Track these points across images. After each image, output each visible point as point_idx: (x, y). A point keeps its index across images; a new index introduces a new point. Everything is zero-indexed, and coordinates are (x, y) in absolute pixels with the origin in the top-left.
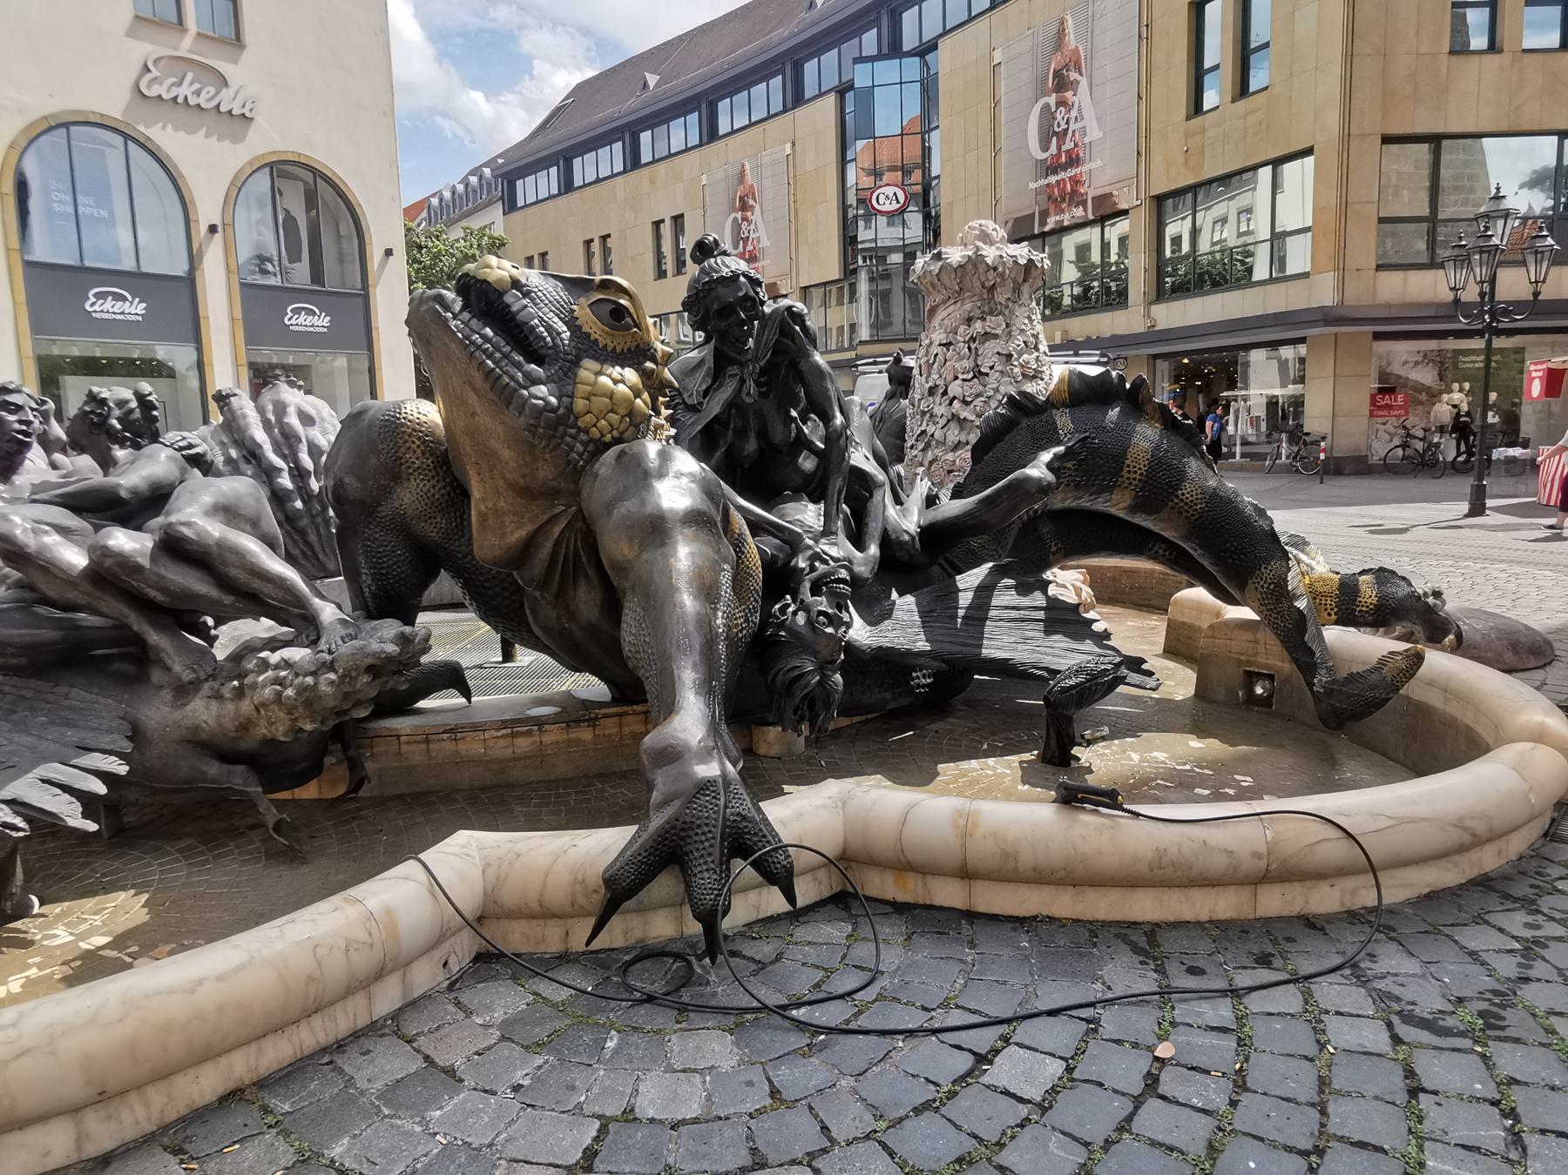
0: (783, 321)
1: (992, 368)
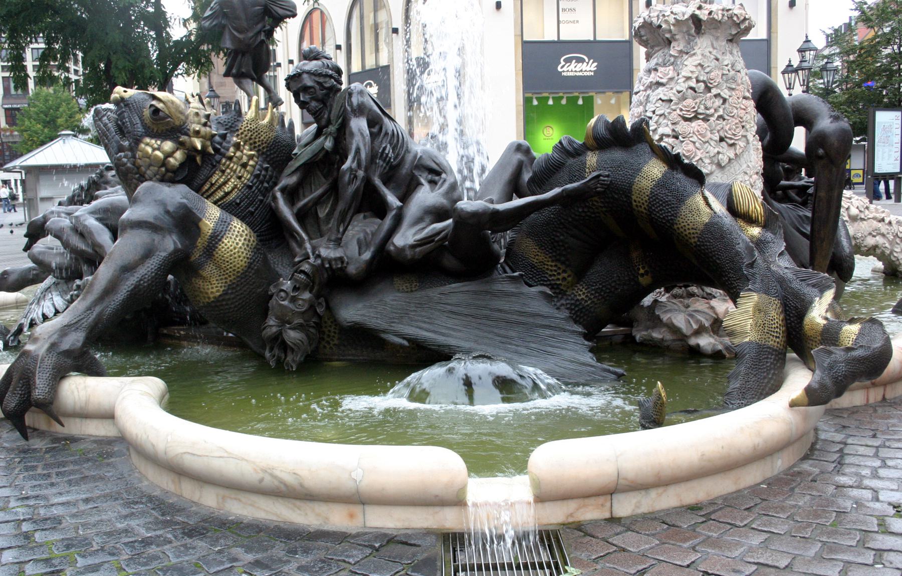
0: (345, 98)
1: (654, 112)
